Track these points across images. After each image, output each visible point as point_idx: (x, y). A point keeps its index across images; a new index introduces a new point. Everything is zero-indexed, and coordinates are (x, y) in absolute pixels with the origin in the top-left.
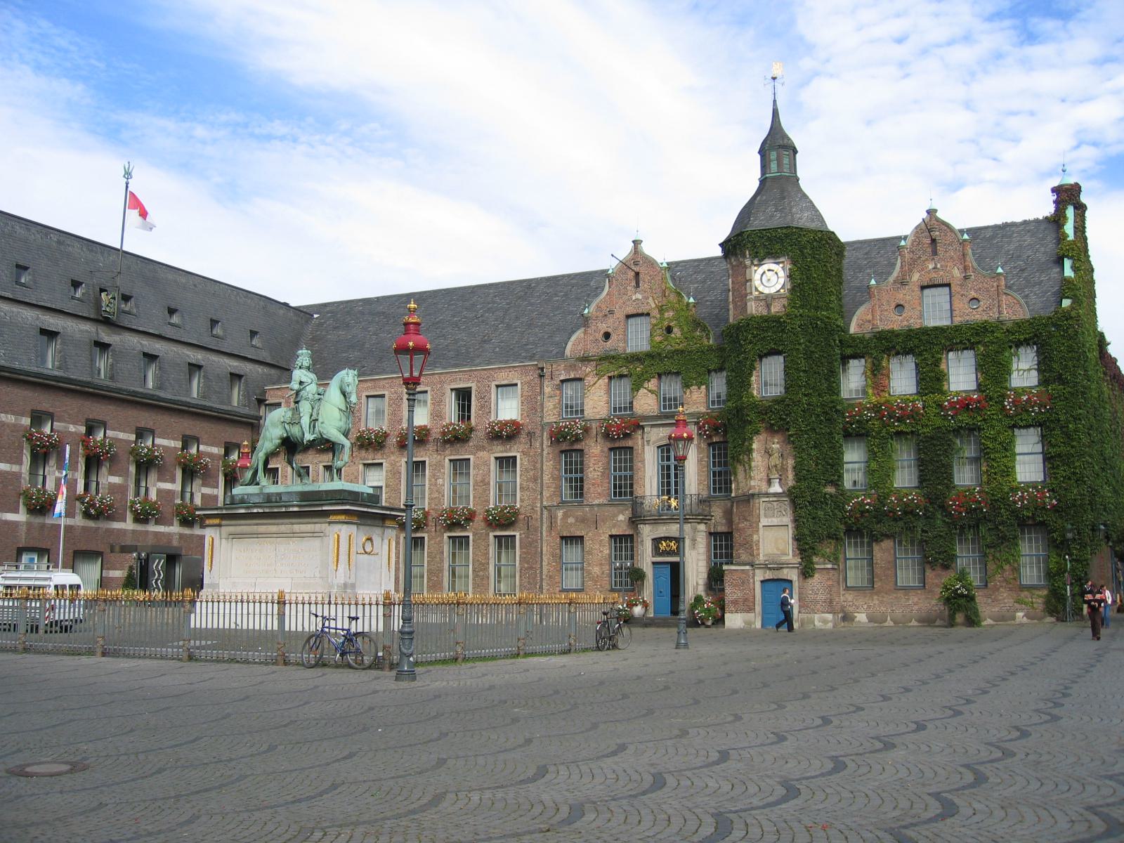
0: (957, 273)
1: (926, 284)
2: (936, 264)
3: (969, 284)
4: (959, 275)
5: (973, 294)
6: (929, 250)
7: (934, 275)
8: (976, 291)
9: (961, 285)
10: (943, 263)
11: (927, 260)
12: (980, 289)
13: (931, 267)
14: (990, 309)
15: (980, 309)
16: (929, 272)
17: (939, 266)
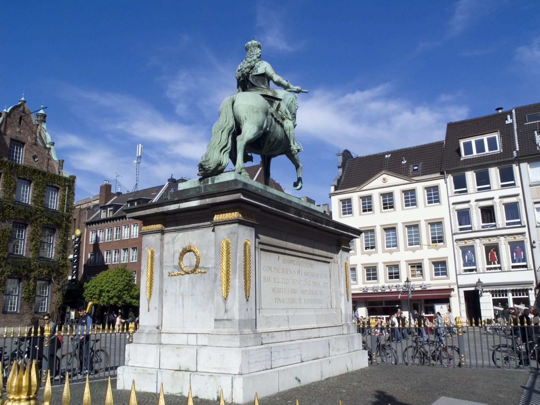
0: (29, 138)
1: (13, 138)
2: (20, 130)
3: (35, 147)
4: (30, 140)
5: (35, 153)
6: (18, 121)
7: (18, 135)
8: (37, 152)
9: (31, 147)
10: (24, 131)
11: (16, 125)
12: (39, 152)
13: (18, 130)
14: (42, 164)
15: (37, 162)
16: (16, 132)
17: (22, 132)
